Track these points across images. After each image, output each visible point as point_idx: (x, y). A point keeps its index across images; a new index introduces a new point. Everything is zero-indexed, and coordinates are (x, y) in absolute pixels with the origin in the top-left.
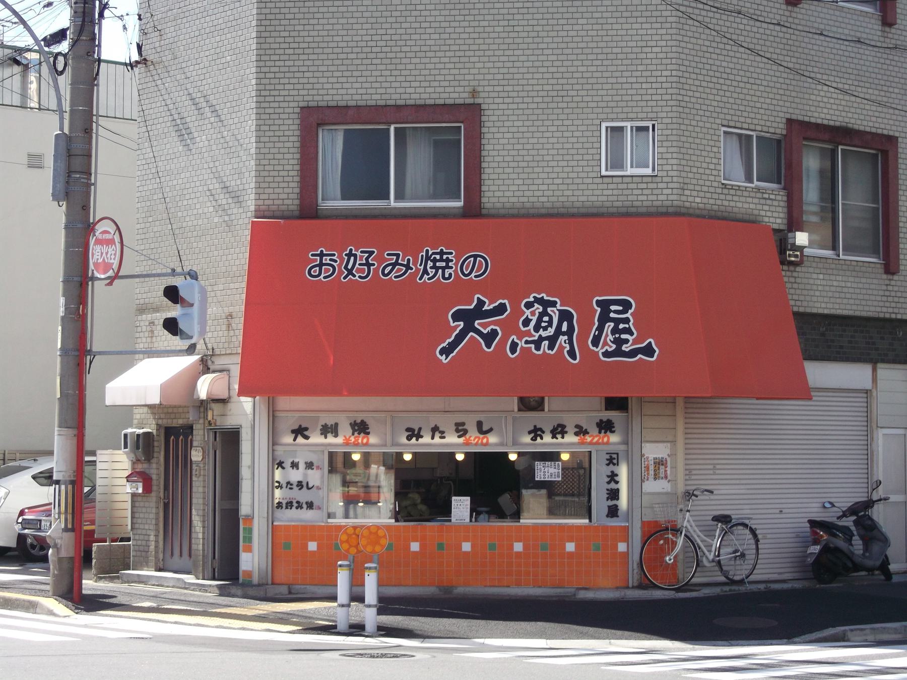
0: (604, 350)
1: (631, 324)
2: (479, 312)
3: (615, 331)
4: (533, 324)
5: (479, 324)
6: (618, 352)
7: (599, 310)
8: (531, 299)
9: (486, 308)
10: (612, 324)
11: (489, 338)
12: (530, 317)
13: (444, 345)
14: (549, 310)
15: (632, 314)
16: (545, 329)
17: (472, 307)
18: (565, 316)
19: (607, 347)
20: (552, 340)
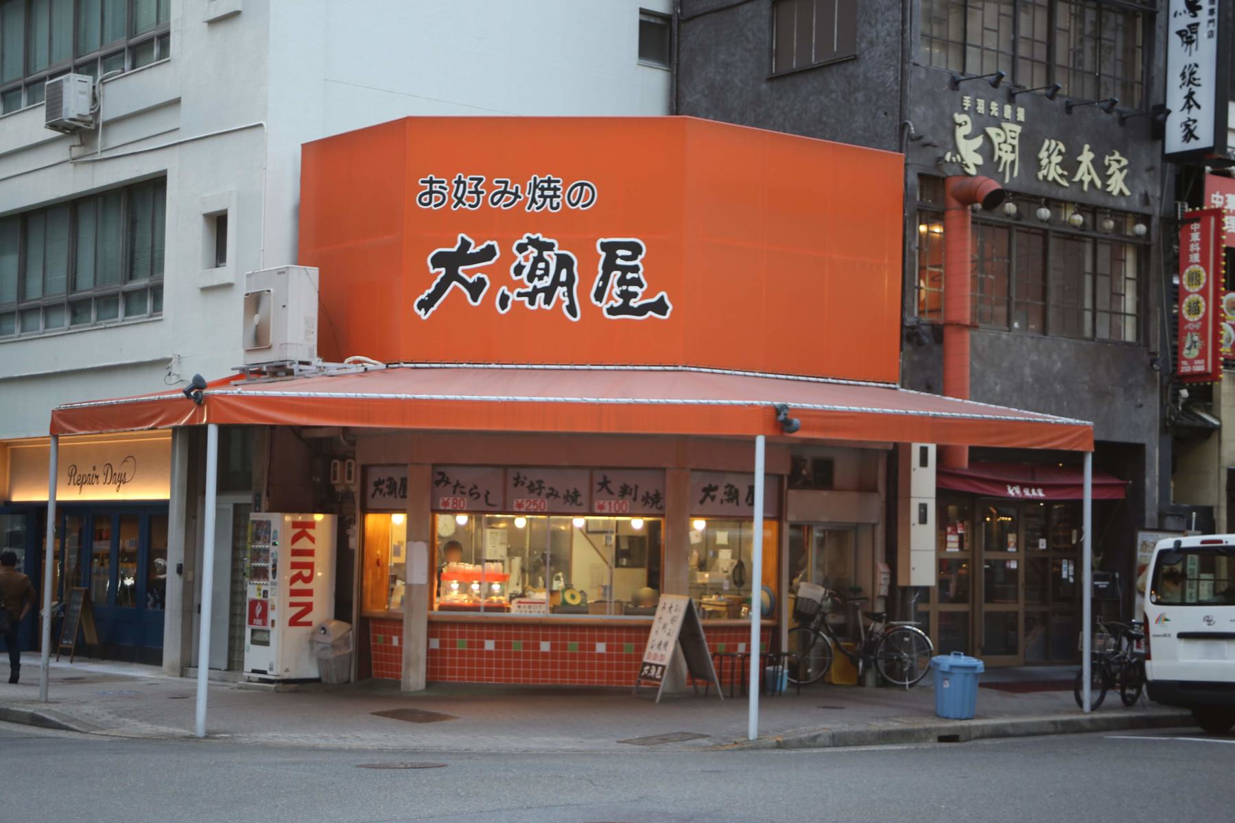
0: (608, 306)
1: (640, 272)
2: (462, 257)
3: (622, 281)
4: (526, 271)
6: (625, 309)
7: (603, 255)
8: (525, 241)
9: (471, 250)
10: (618, 274)
11: (476, 288)
12: (523, 263)
13: (423, 297)
14: (545, 254)
15: (642, 261)
16: (541, 278)
17: (455, 249)
18: (564, 262)
19: (612, 303)
20: (549, 292)
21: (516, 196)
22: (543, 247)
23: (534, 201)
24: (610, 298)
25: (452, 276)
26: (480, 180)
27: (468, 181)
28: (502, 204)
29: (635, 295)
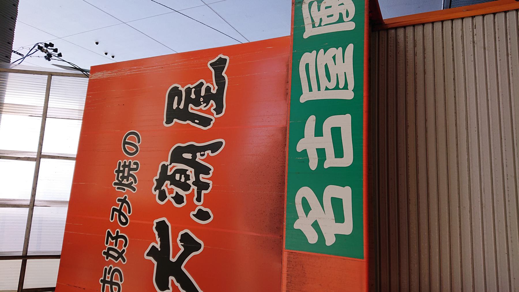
0: (215, 113)
1: (191, 86)
3: (197, 103)
5: (174, 257)
6: (218, 98)
8: (157, 193)
9: (158, 246)
10: (191, 105)
11: (190, 245)
12: (174, 195)
14: (169, 173)
15: (183, 87)
16: (187, 178)
17: (155, 263)
18: (177, 157)
21: (124, 201)
22: (164, 177)
23: (129, 186)
24: (208, 112)
25: (175, 269)
26: (109, 234)
27: (108, 246)
28: (127, 215)
29: (208, 89)
